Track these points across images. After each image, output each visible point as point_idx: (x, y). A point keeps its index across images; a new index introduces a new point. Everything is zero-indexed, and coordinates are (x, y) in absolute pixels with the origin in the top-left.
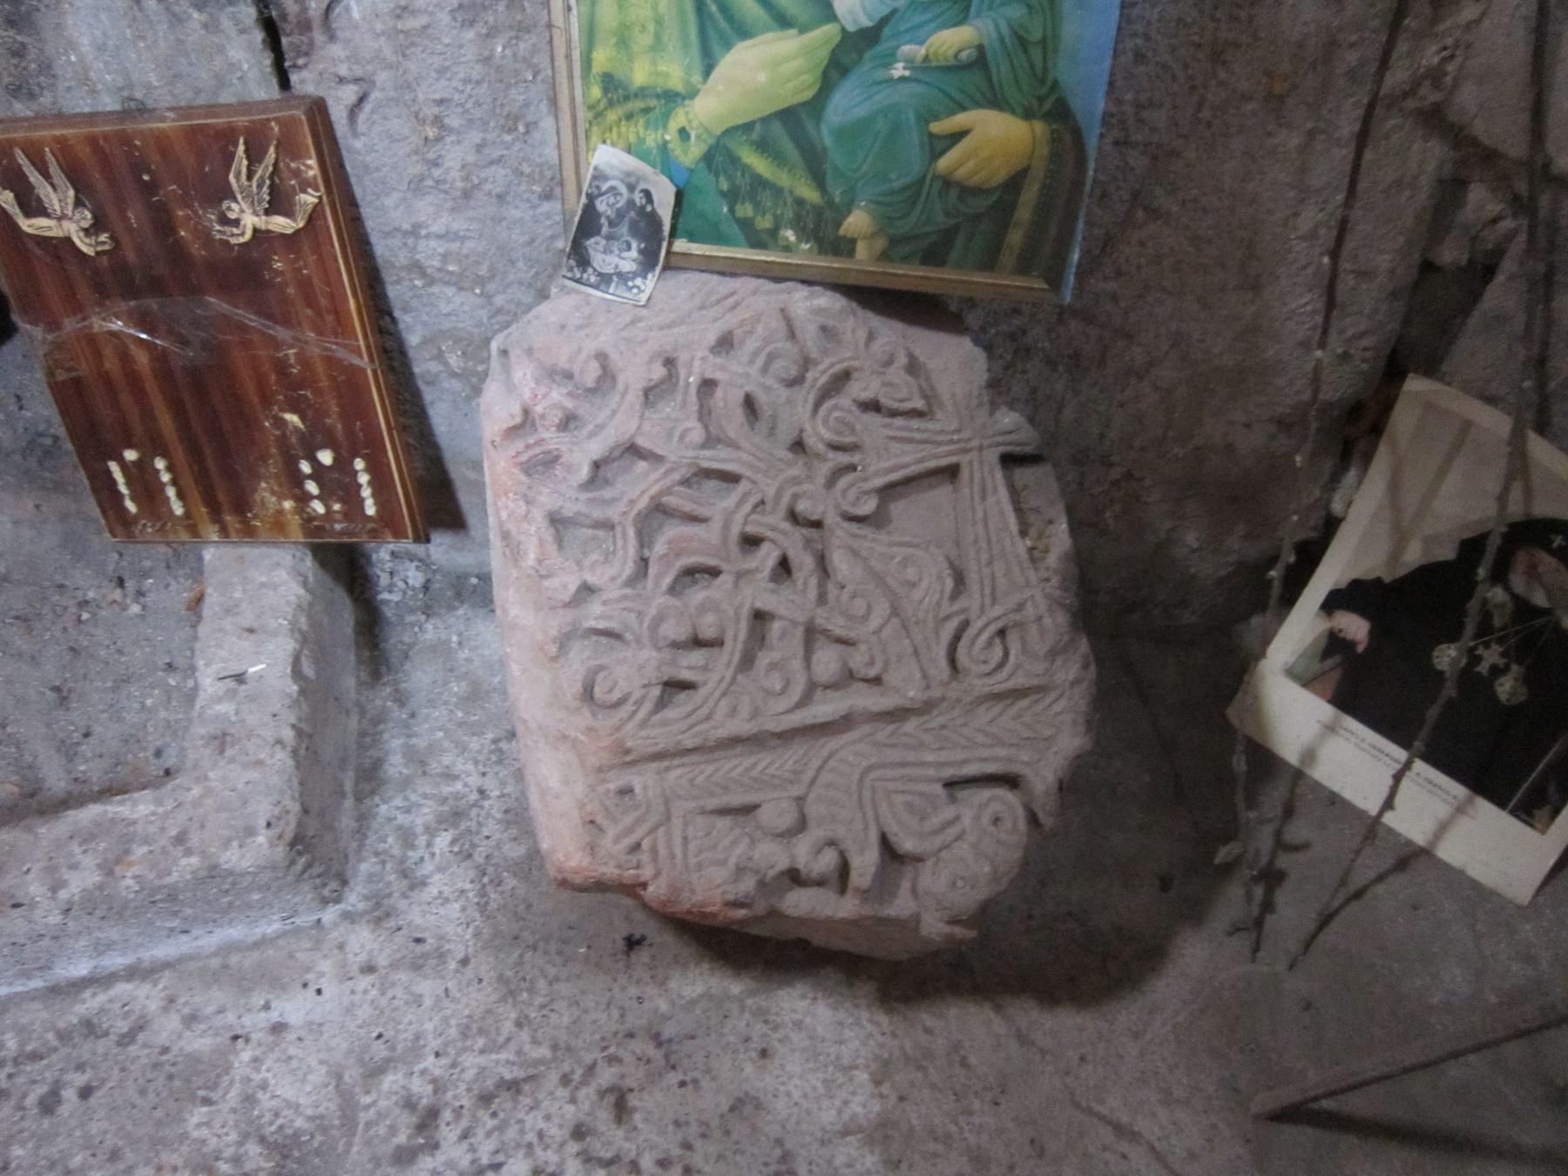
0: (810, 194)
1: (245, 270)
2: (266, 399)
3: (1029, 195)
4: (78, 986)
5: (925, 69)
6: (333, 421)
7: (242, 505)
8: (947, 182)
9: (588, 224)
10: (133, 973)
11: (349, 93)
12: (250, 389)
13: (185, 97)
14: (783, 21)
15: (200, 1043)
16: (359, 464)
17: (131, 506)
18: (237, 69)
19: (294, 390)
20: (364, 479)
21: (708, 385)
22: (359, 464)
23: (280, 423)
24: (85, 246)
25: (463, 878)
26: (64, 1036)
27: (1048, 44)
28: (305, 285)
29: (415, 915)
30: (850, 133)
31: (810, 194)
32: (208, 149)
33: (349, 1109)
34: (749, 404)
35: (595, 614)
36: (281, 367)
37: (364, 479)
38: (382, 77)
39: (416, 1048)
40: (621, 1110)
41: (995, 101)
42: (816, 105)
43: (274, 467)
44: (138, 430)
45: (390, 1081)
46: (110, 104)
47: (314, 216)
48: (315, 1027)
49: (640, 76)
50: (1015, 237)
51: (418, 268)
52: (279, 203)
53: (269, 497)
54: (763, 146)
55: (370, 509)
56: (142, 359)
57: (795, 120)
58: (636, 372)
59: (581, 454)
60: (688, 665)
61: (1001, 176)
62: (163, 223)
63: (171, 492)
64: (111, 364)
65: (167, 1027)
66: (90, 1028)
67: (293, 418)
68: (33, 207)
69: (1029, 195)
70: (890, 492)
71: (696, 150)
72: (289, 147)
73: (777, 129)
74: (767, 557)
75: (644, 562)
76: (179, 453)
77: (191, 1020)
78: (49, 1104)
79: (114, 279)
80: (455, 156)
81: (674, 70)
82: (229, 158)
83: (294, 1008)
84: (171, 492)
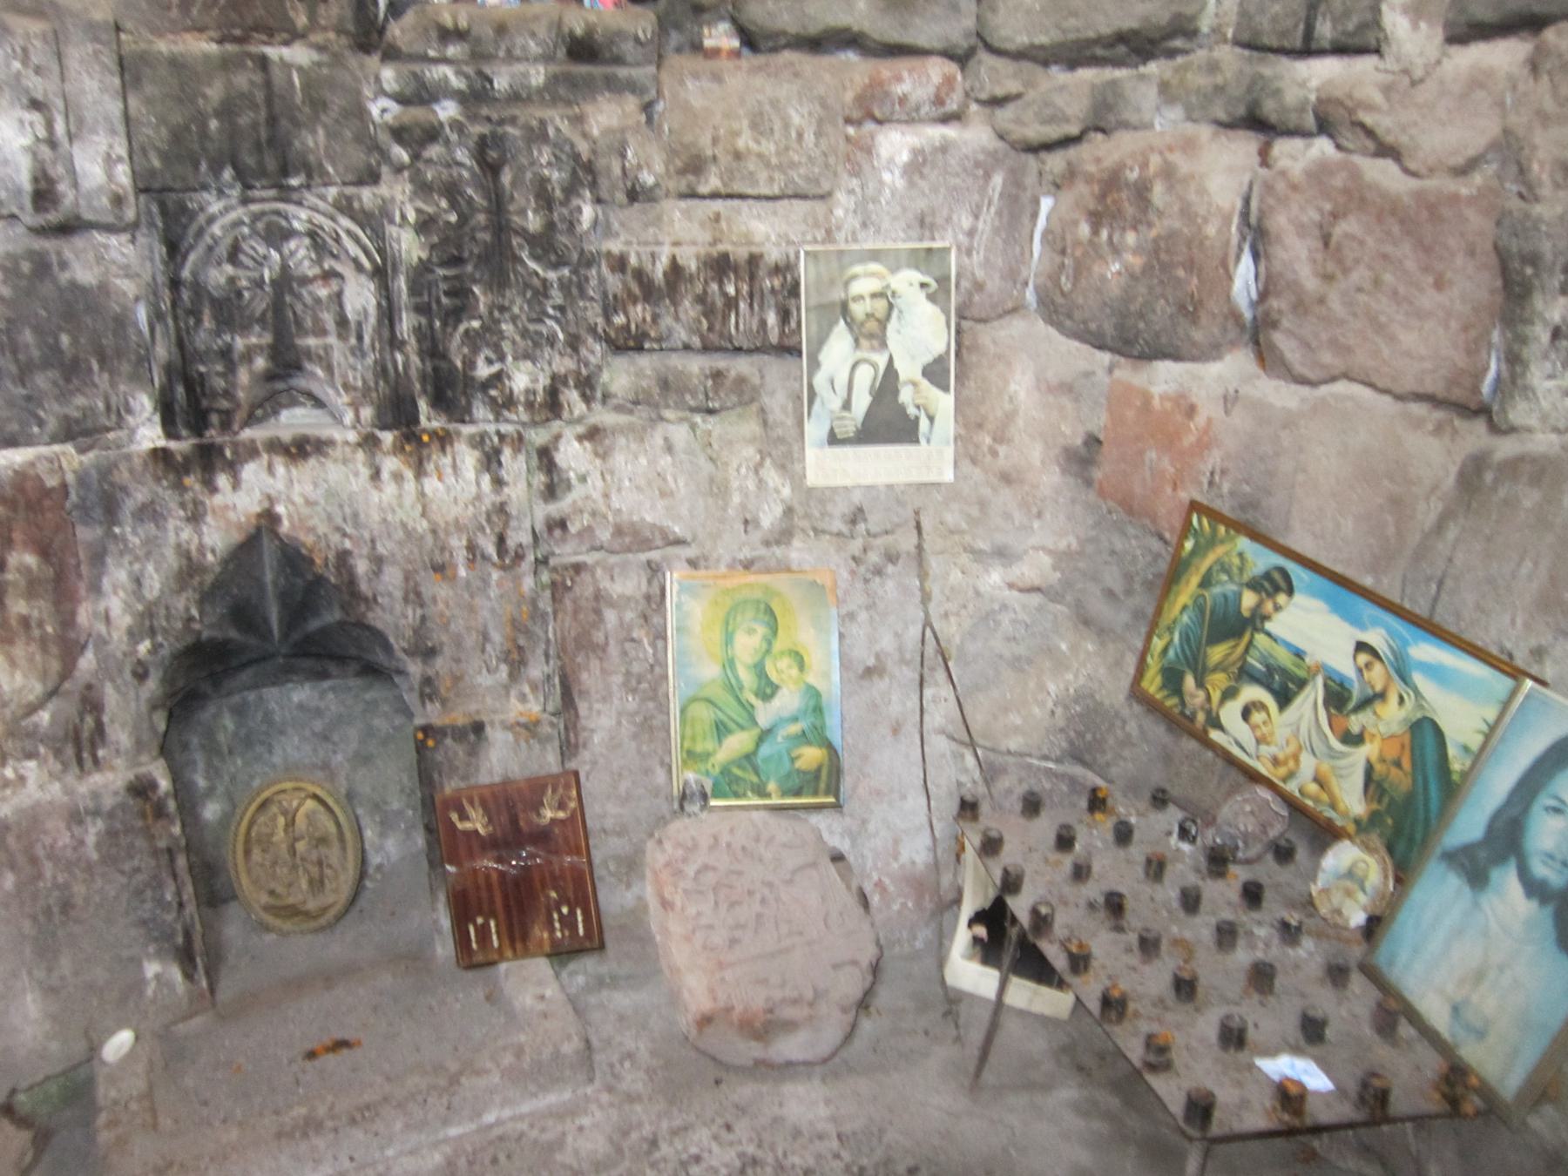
0: (755, 779)
1: (542, 837)
2: (544, 886)
3: (824, 773)
4: (490, 1127)
5: (788, 738)
6: (571, 894)
7: (525, 937)
8: (799, 771)
9: (683, 797)
10: (512, 1119)
11: (587, 767)
12: (538, 885)
13: (527, 774)
14: (742, 728)
15: (549, 1136)
16: (579, 912)
17: (474, 946)
18: (550, 761)
19: (555, 881)
20: (580, 918)
21: (729, 845)
22: (579, 912)
23: (548, 897)
24: (482, 831)
25: (641, 1074)
26: (491, 1143)
27: (823, 727)
28: (566, 839)
29: (623, 1086)
30: (767, 760)
31: (755, 779)
32: (536, 789)
33: (619, 1151)
34: (744, 848)
35: (704, 921)
36: (552, 873)
37: (580, 918)
38: (601, 761)
39: (640, 1125)
40: (729, 1128)
41: (809, 743)
42: (755, 752)
43: (542, 918)
44: (485, 907)
45: (634, 1136)
46: (497, 779)
47: (574, 811)
48: (596, 1126)
49: (699, 748)
50: (822, 785)
51: (604, 831)
52: (562, 806)
53: (539, 933)
54: (739, 767)
55: (581, 931)
56: (494, 876)
57: (749, 758)
58: (705, 842)
59: (690, 870)
60: (738, 934)
61: (814, 766)
62: (514, 821)
63: (495, 937)
64: (481, 881)
65: (534, 1134)
66: (501, 1138)
67: (553, 895)
68: (464, 817)
69: (824, 773)
70: (794, 872)
71: (717, 770)
72: (567, 787)
73: (745, 763)
74: (758, 896)
75: (716, 903)
76: (502, 916)
77: (543, 1130)
78: (495, 1161)
79: (491, 844)
80: (624, 786)
81: (709, 745)
82: (543, 793)
83: (585, 1121)
84: (495, 937)
